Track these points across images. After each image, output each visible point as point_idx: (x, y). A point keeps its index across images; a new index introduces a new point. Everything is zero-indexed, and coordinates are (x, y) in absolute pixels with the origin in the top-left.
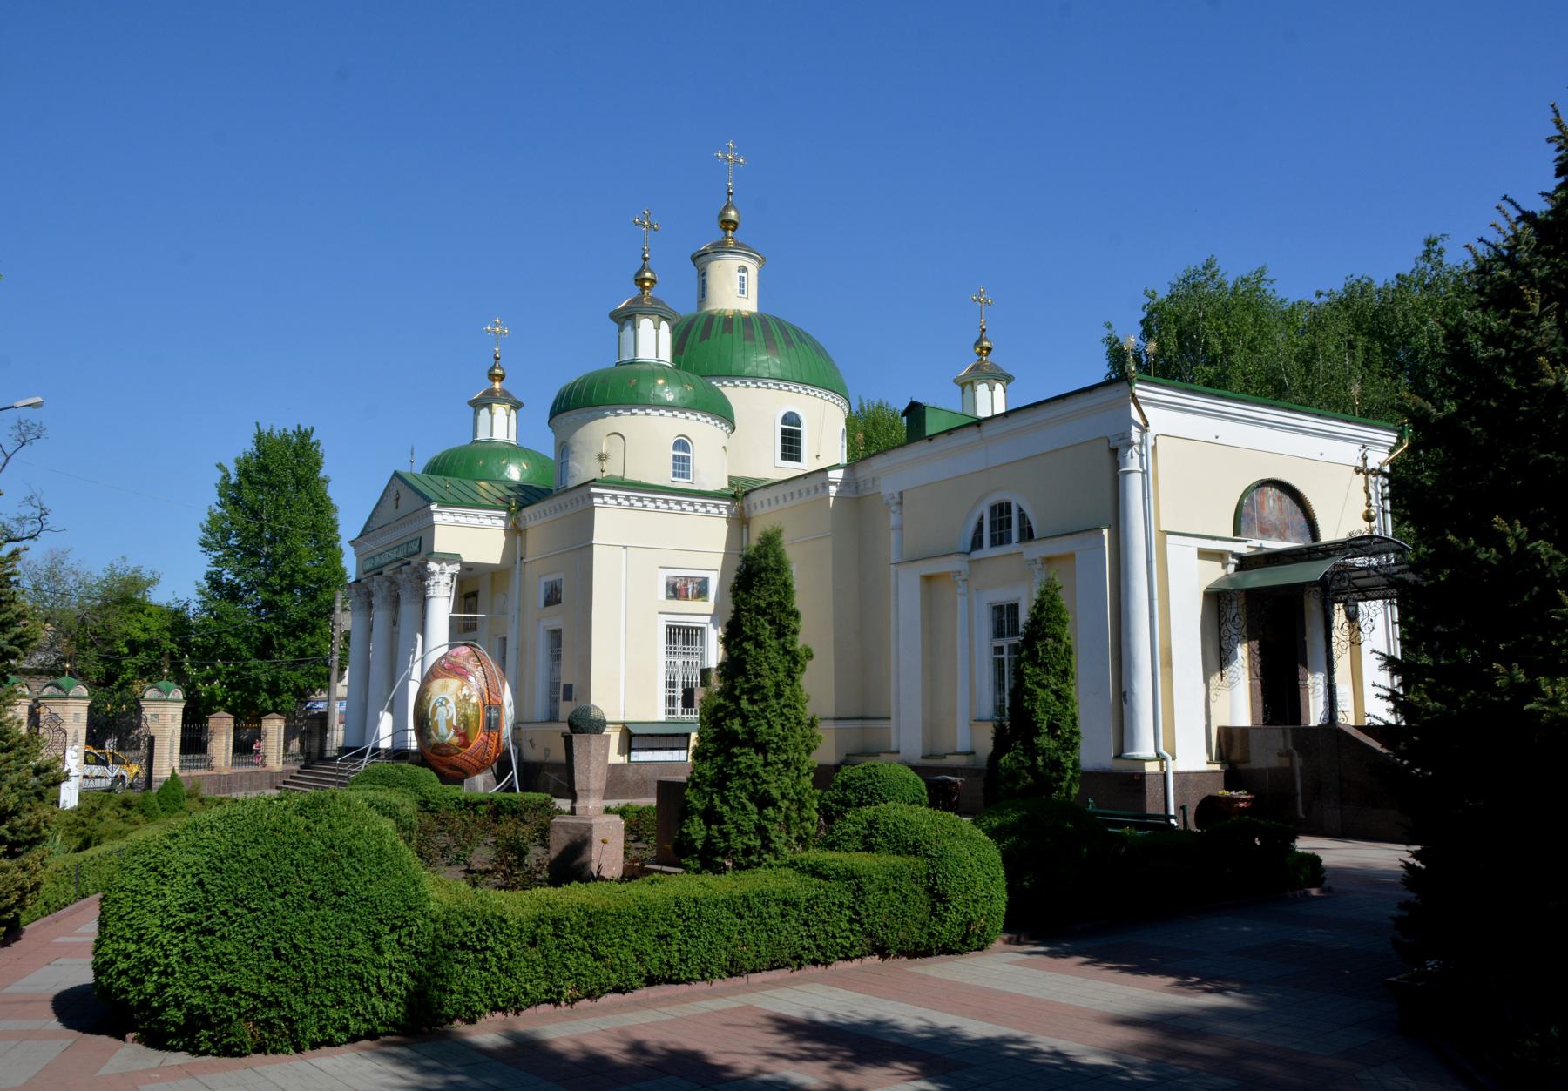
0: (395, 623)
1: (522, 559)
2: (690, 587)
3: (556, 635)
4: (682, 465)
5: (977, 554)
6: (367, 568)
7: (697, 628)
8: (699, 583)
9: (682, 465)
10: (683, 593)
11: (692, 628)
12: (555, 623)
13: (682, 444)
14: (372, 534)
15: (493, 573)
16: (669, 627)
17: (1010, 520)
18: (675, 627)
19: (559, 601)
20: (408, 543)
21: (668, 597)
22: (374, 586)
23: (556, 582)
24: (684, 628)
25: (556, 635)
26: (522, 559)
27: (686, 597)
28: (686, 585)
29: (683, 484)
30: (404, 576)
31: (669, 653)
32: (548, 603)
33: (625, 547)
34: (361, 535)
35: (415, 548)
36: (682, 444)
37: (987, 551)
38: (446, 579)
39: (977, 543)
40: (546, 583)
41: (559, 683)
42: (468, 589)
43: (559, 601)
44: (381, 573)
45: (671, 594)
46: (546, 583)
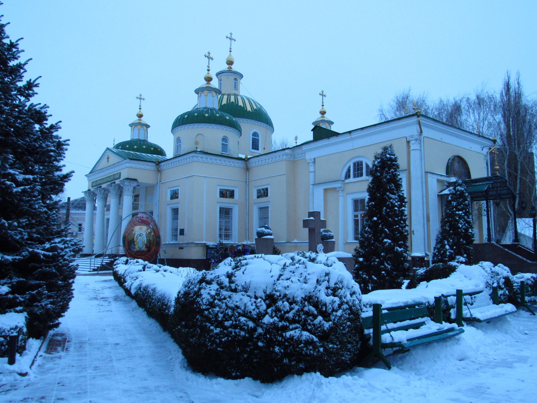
0: (120, 204)
1: (160, 182)
2: (228, 193)
3: (175, 211)
4: (225, 147)
5: (347, 181)
6: (93, 185)
7: (230, 209)
8: (231, 192)
9: (225, 147)
10: (225, 195)
11: (228, 208)
12: (175, 206)
13: (225, 139)
14: (96, 172)
15: (146, 188)
16: (221, 208)
17: (362, 168)
18: (222, 208)
19: (178, 197)
20: (114, 175)
21: (220, 197)
22: (97, 192)
23: (175, 190)
24: (225, 208)
25: (175, 211)
26: (160, 182)
27: (226, 197)
28: (226, 192)
29: (225, 154)
30: (113, 187)
31: (220, 218)
32: (172, 198)
33: (205, 177)
34: (91, 173)
35: (117, 177)
36: (225, 139)
37: (352, 179)
38: (131, 189)
39: (348, 176)
40: (171, 191)
41: (177, 229)
42: (136, 193)
43: (178, 197)
44: (101, 187)
45: (221, 195)
46: (171, 191)
